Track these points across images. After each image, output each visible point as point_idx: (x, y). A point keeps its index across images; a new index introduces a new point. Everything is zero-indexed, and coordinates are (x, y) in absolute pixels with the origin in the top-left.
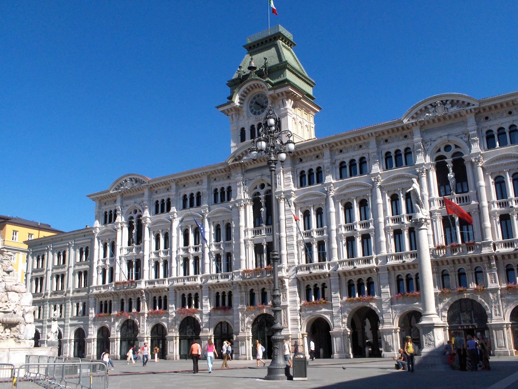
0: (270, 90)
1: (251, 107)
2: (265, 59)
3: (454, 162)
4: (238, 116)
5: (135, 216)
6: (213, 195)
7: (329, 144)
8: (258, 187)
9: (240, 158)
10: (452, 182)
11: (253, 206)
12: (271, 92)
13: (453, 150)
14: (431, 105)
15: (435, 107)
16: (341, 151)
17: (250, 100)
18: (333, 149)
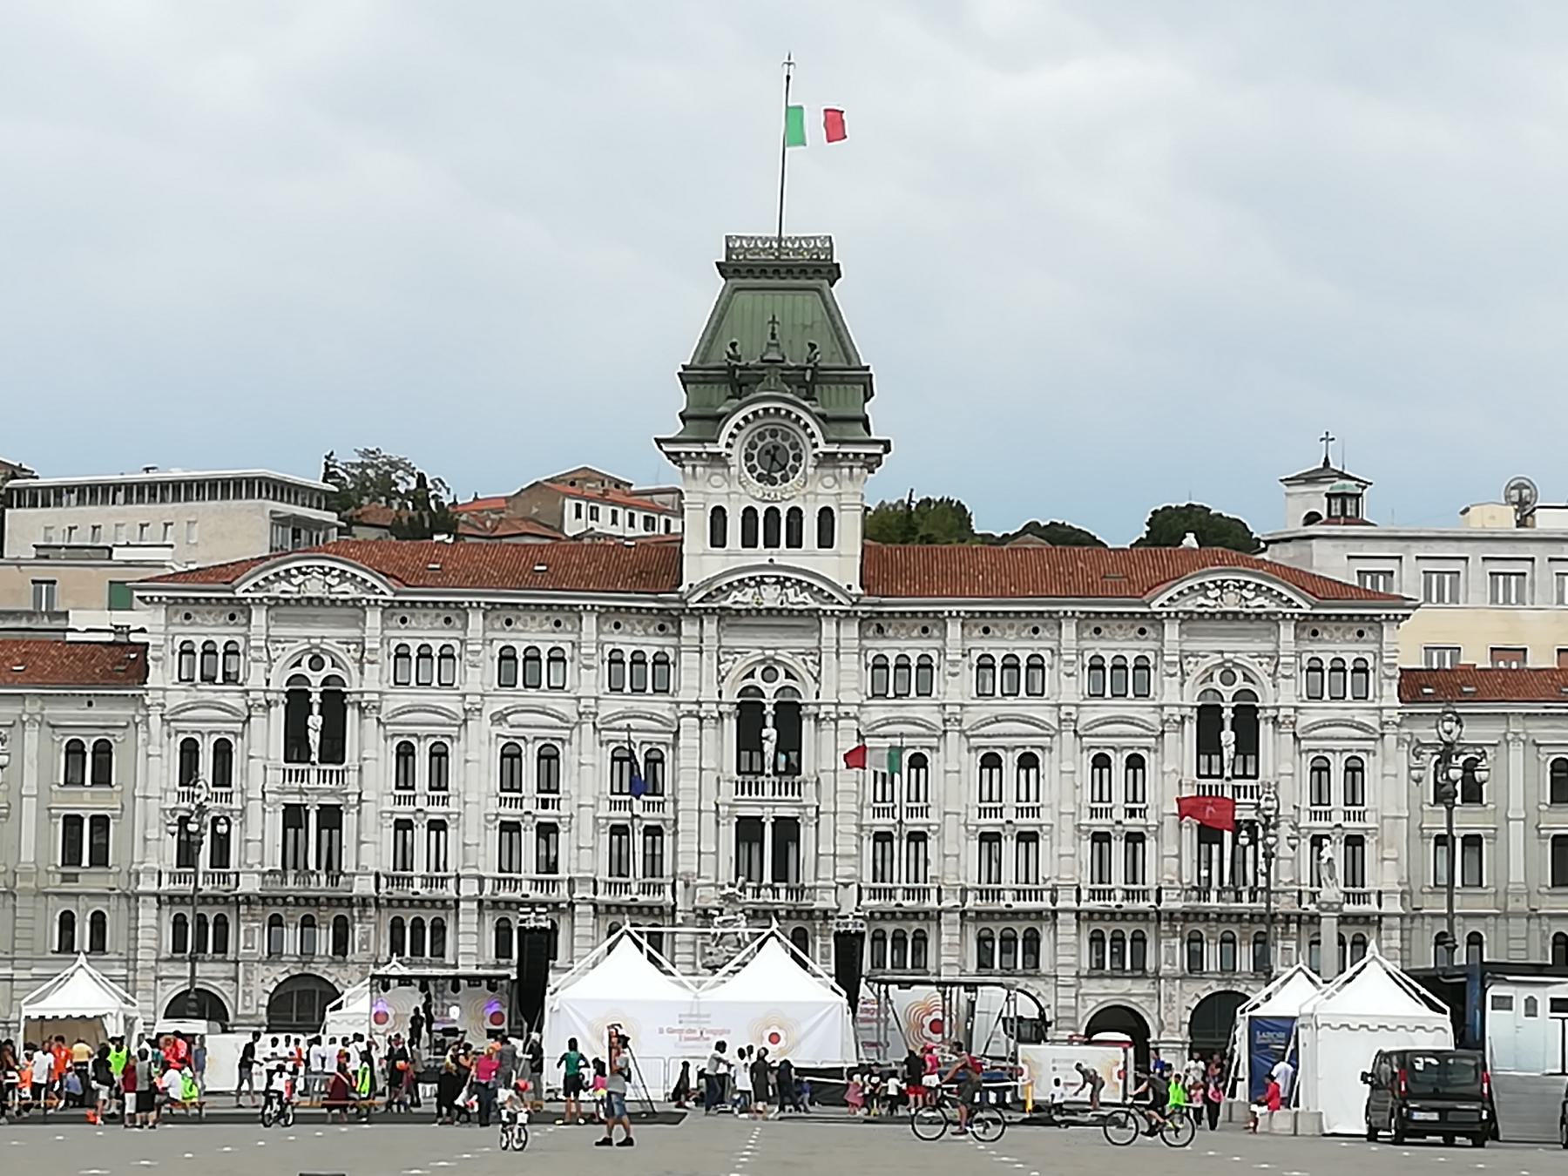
1: (749, 457)
2: (813, 346)
3: (1234, 710)
5: (316, 679)
10: (1229, 752)
11: (738, 719)
13: (1240, 684)
14: (1214, 582)
15: (1221, 587)
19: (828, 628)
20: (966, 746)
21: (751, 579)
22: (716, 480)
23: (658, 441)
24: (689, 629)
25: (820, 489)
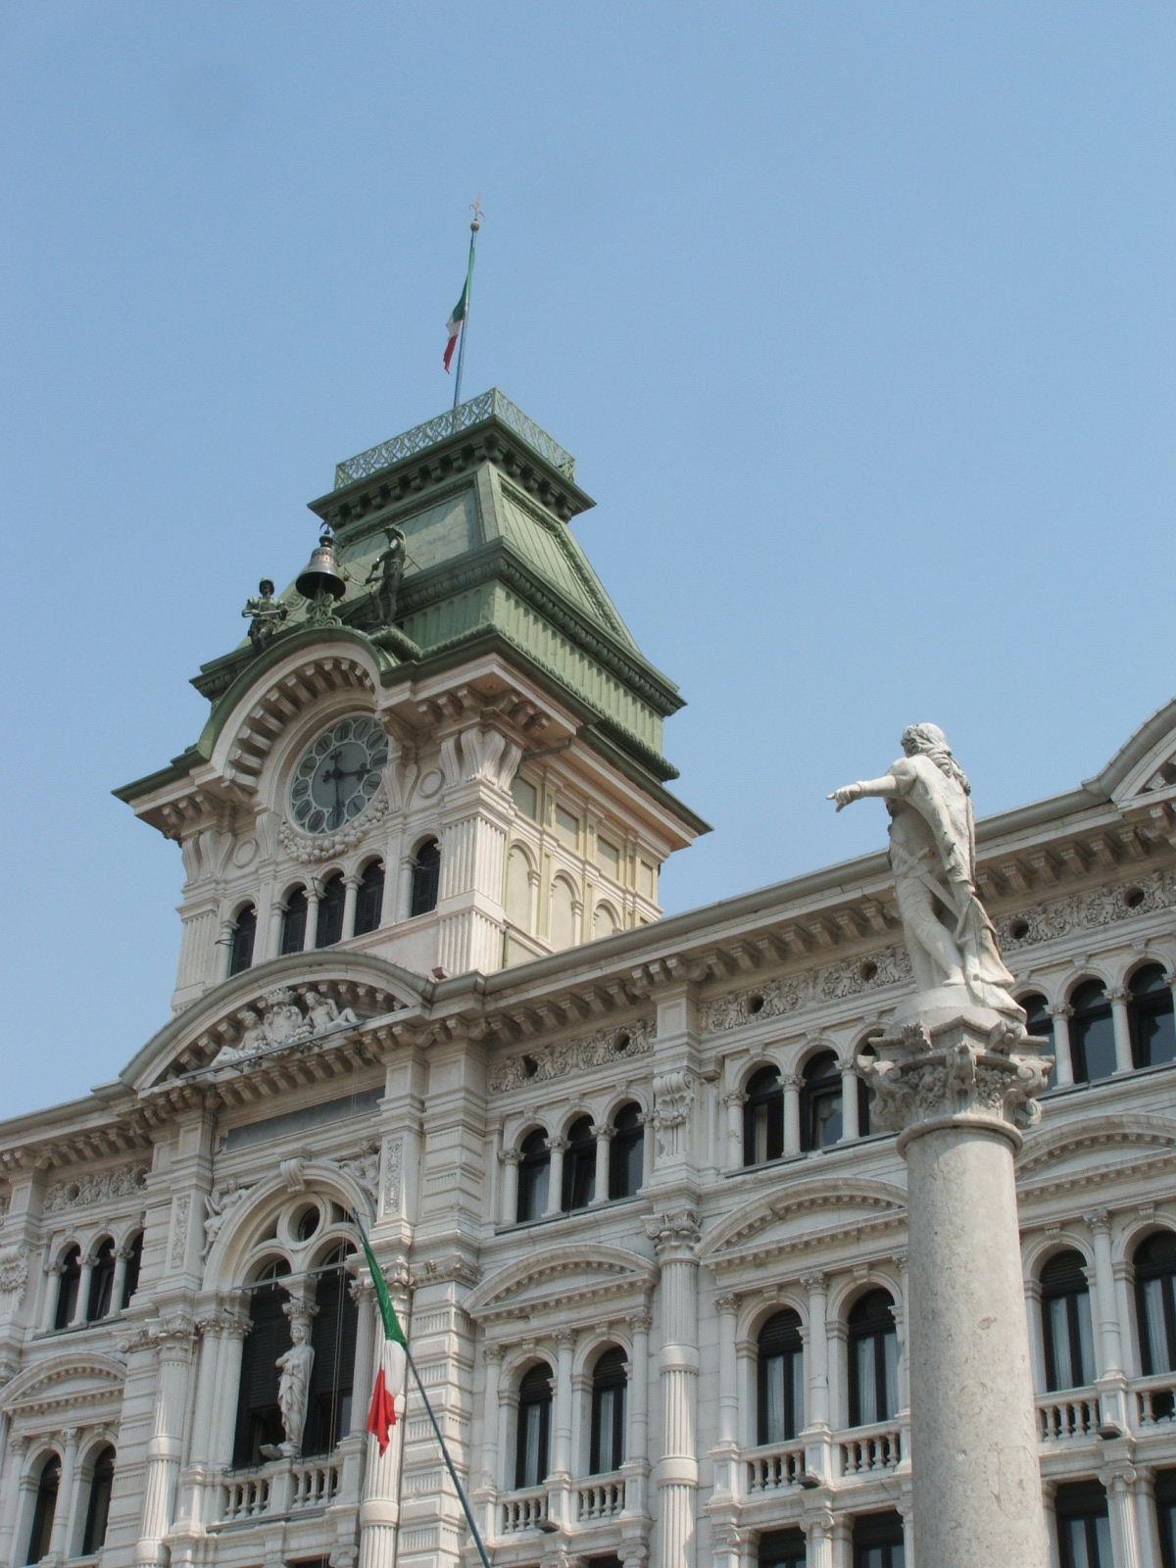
0: (390, 679)
1: (298, 792)
4: (228, 839)
6: (53, 1281)
7: (684, 959)
8: (283, 1228)
9: (200, 1055)
12: (400, 694)
16: (756, 1005)
17: (301, 757)
18: (709, 992)
19: (399, 1083)
20: (707, 1308)
21: (252, 1006)
22: (244, 854)
23: (127, 794)
24: (161, 1157)
25: (417, 803)
